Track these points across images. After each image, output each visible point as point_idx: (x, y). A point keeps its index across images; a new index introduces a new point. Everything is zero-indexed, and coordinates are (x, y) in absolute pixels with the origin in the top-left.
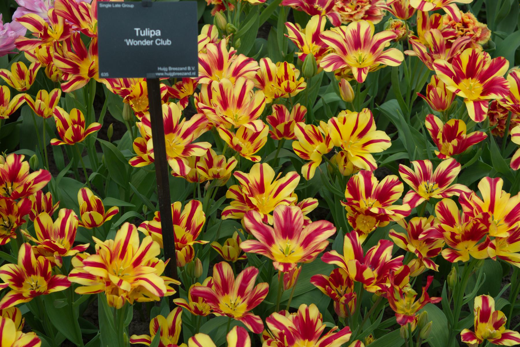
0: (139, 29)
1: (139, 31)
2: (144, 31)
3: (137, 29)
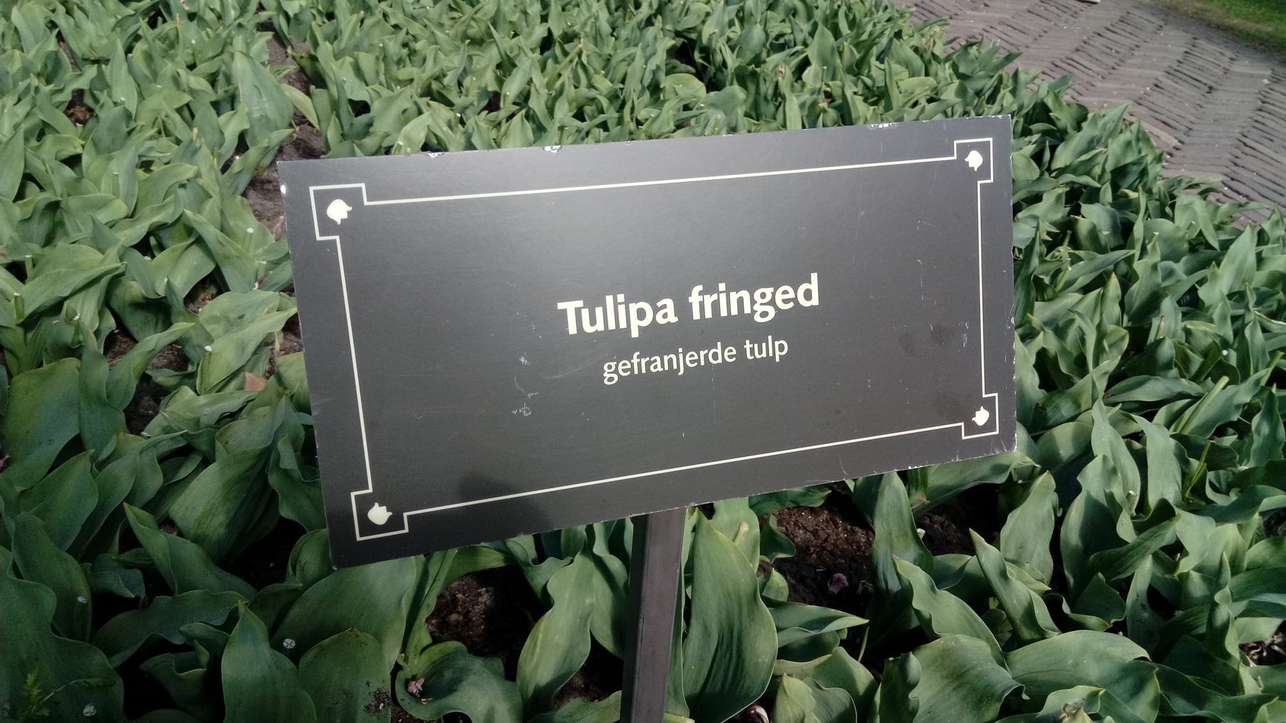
0: (580, 303)
1: (578, 312)
2: (599, 311)
3: (570, 307)
